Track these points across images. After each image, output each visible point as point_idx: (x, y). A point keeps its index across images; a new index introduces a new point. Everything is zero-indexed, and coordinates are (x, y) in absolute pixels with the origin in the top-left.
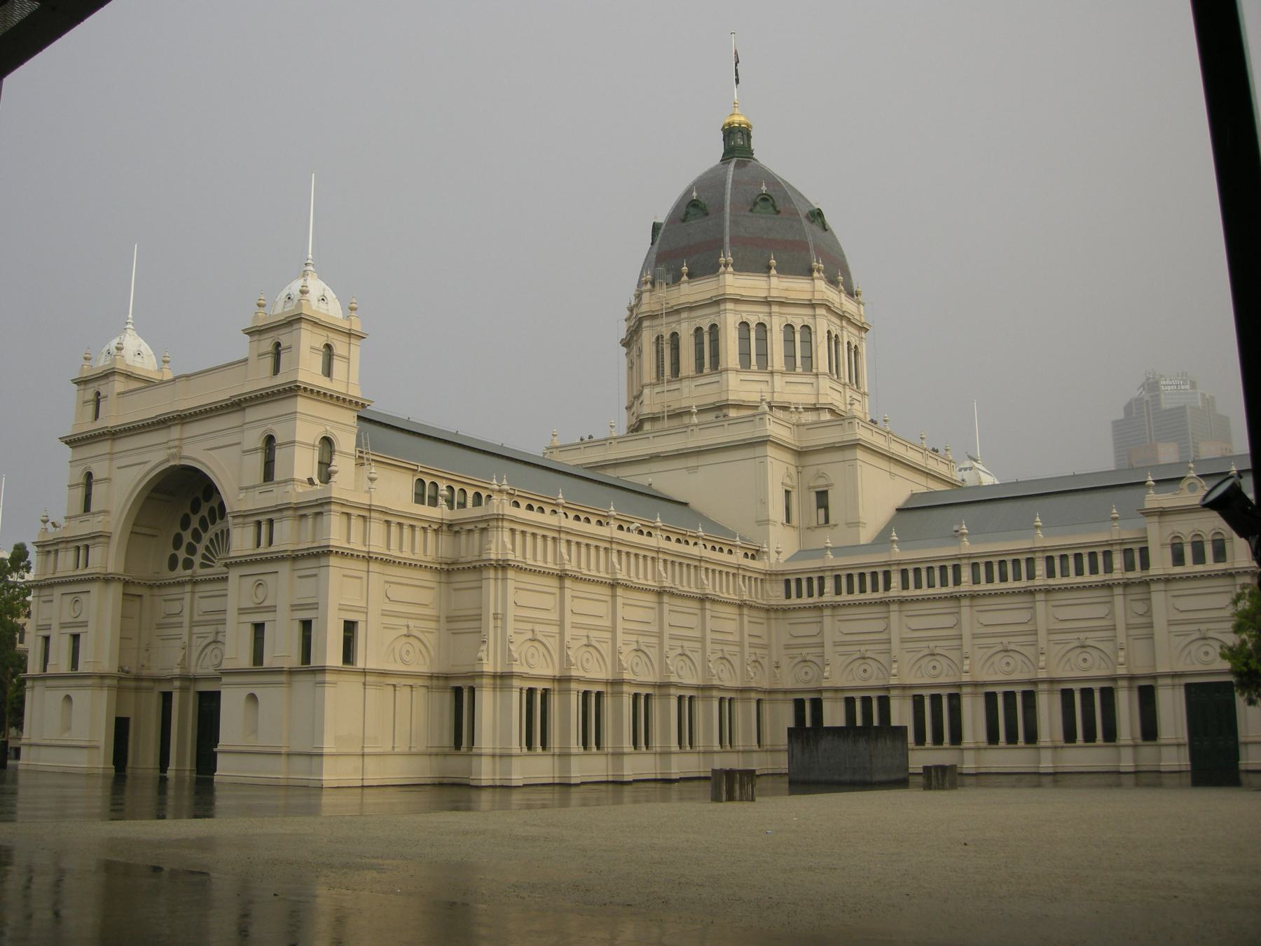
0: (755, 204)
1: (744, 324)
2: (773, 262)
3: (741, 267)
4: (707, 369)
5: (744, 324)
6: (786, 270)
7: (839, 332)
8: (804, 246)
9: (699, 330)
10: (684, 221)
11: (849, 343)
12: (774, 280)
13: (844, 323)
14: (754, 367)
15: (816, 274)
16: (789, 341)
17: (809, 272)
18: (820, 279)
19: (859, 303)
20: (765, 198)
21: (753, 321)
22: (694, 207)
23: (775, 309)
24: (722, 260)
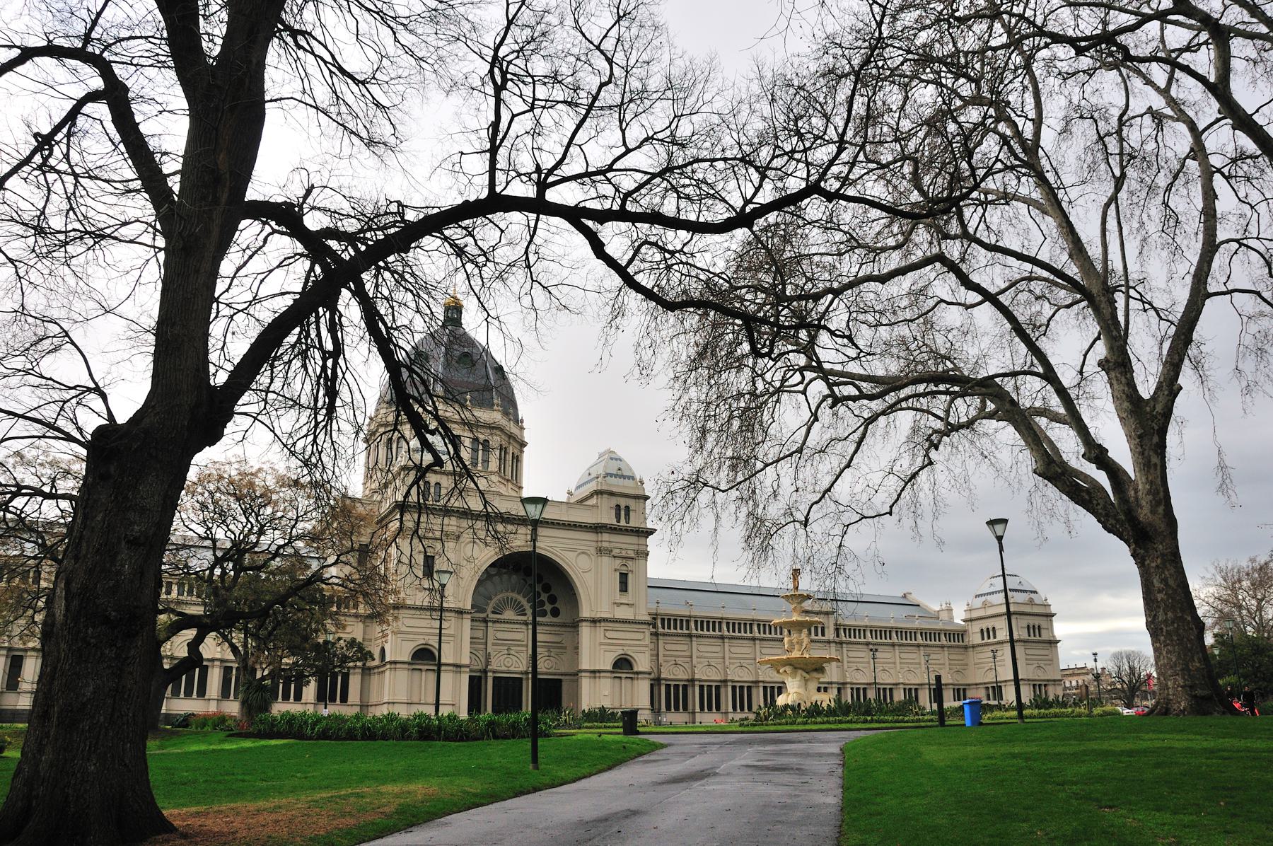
20: (466, 355)
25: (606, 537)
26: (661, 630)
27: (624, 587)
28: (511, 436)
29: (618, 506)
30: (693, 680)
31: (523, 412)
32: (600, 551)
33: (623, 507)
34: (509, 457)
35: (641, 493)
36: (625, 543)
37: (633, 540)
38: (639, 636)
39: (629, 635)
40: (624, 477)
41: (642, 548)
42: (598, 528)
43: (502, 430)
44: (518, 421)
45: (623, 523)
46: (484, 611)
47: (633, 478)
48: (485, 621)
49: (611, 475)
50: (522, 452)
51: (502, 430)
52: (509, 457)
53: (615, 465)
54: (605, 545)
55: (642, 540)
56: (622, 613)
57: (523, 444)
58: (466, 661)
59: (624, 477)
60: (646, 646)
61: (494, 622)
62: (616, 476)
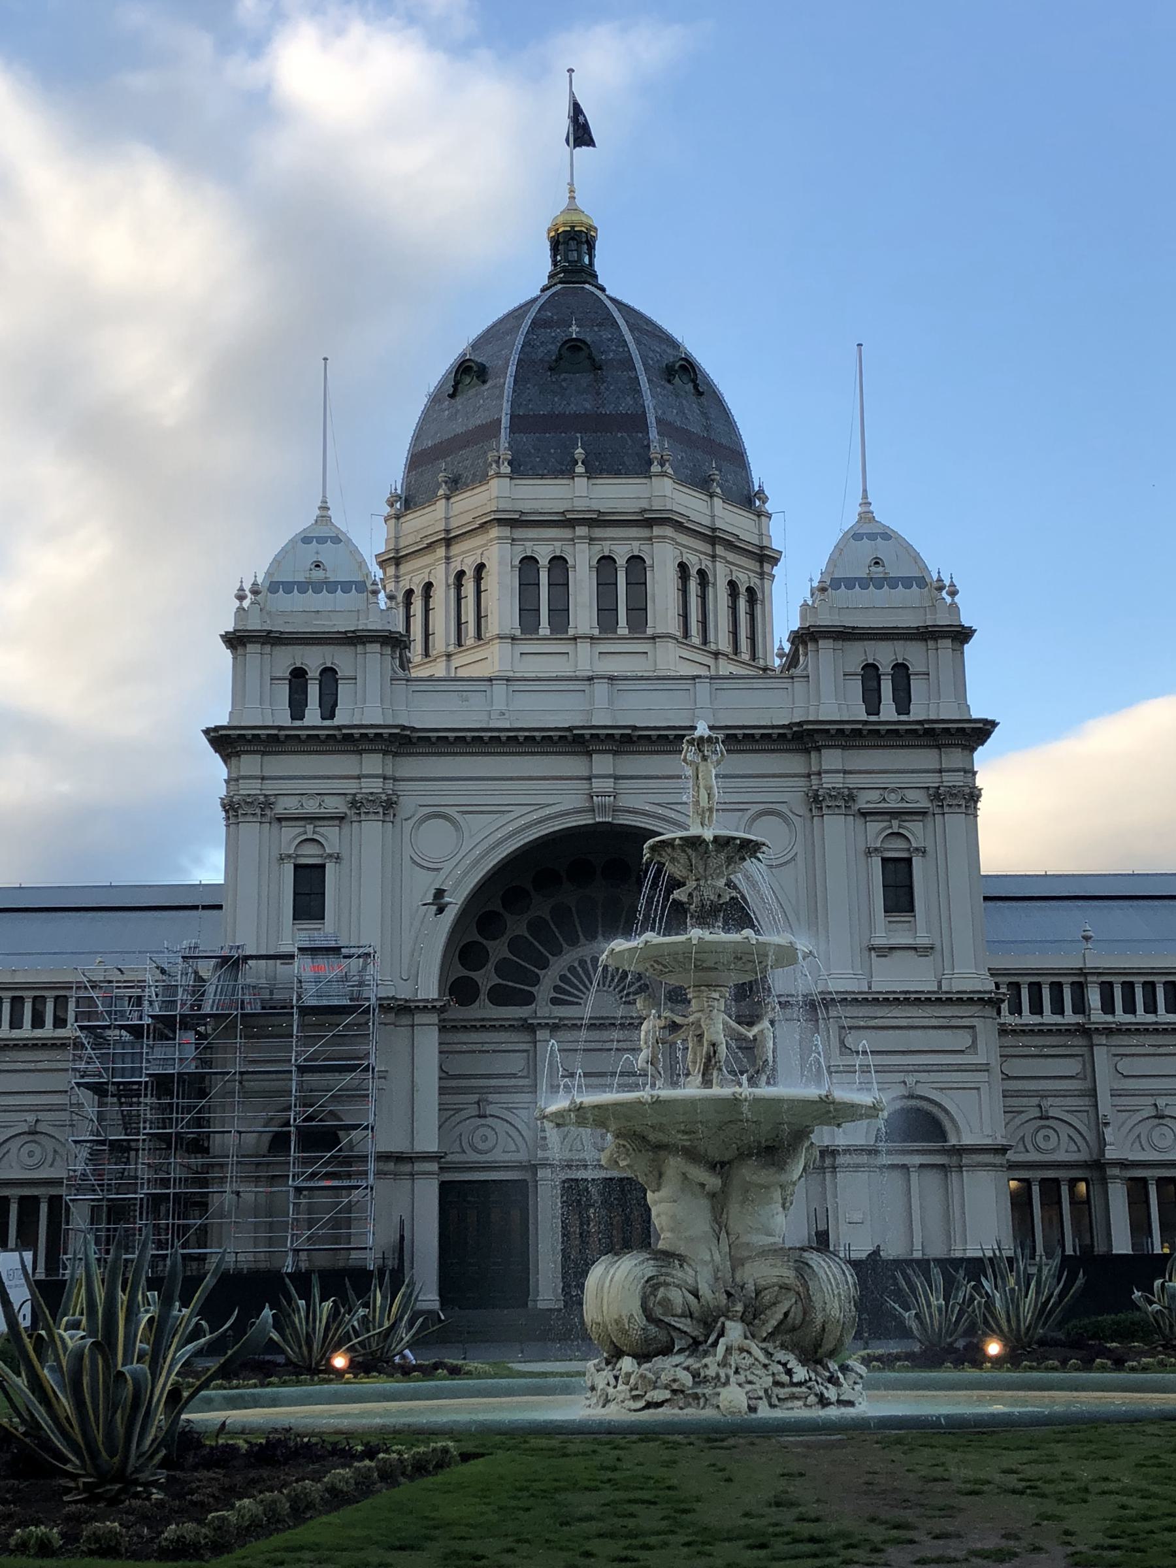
0: (560, 357)
1: (529, 562)
2: (579, 452)
3: (519, 468)
4: (470, 640)
5: (529, 562)
6: (601, 466)
7: (706, 563)
8: (637, 422)
9: (461, 574)
10: (452, 396)
11: (732, 585)
12: (581, 483)
13: (720, 550)
14: (544, 630)
15: (656, 468)
16: (605, 585)
17: (641, 467)
18: (663, 474)
19: (759, 514)
20: (575, 346)
21: (543, 555)
22: (468, 373)
23: (581, 531)
24: (491, 456)
25: (832, 759)
26: (1098, 1016)
27: (899, 894)
28: (713, 537)
29: (871, 672)
30: (1097, 1168)
31: (761, 471)
32: (816, 801)
33: (885, 668)
34: (720, 597)
35: (943, 620)
36: (905, 772)
37: (925, 758)
38: (962, 1040)
39: (917, 1039)
40: (893, 582)
41: (950, 779)
42: (803, 738)
43: (679, 526)
44: (749, 500)
45: (888, 711)
46: (528, 999)
47: (922, 582)
48: (529, 1028)
49: (850, 583)
50: (762, 575)
51: (679, 526)
52: (720, 597)
53: (866, 551)
54: (830, 781)
55: (953, 758)
56: (892, 976)
57: (765, 557)
58: (428, 1142)
59: (893, 582)
60: (985, 1068)
61: (554, 1028)
62: (864, 583)
